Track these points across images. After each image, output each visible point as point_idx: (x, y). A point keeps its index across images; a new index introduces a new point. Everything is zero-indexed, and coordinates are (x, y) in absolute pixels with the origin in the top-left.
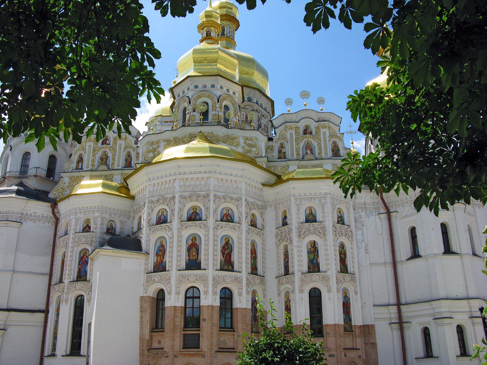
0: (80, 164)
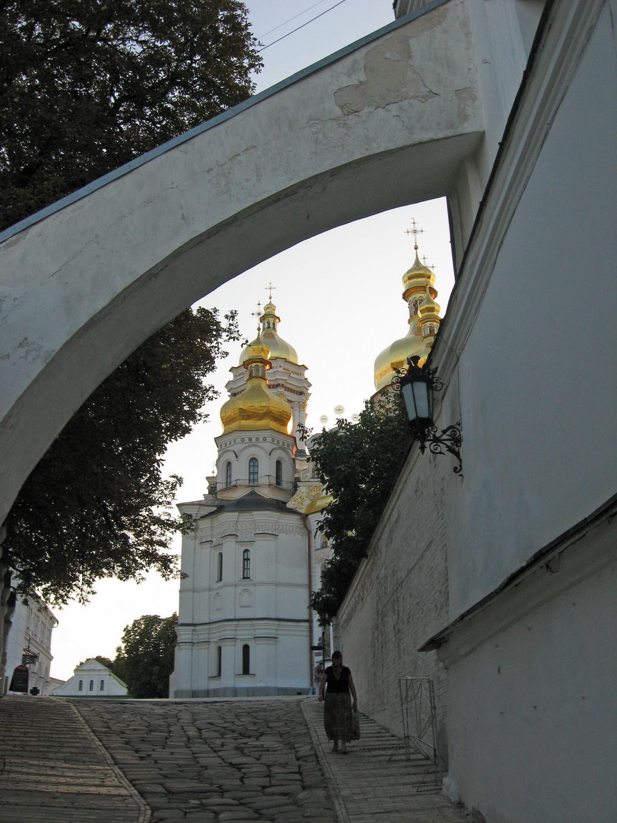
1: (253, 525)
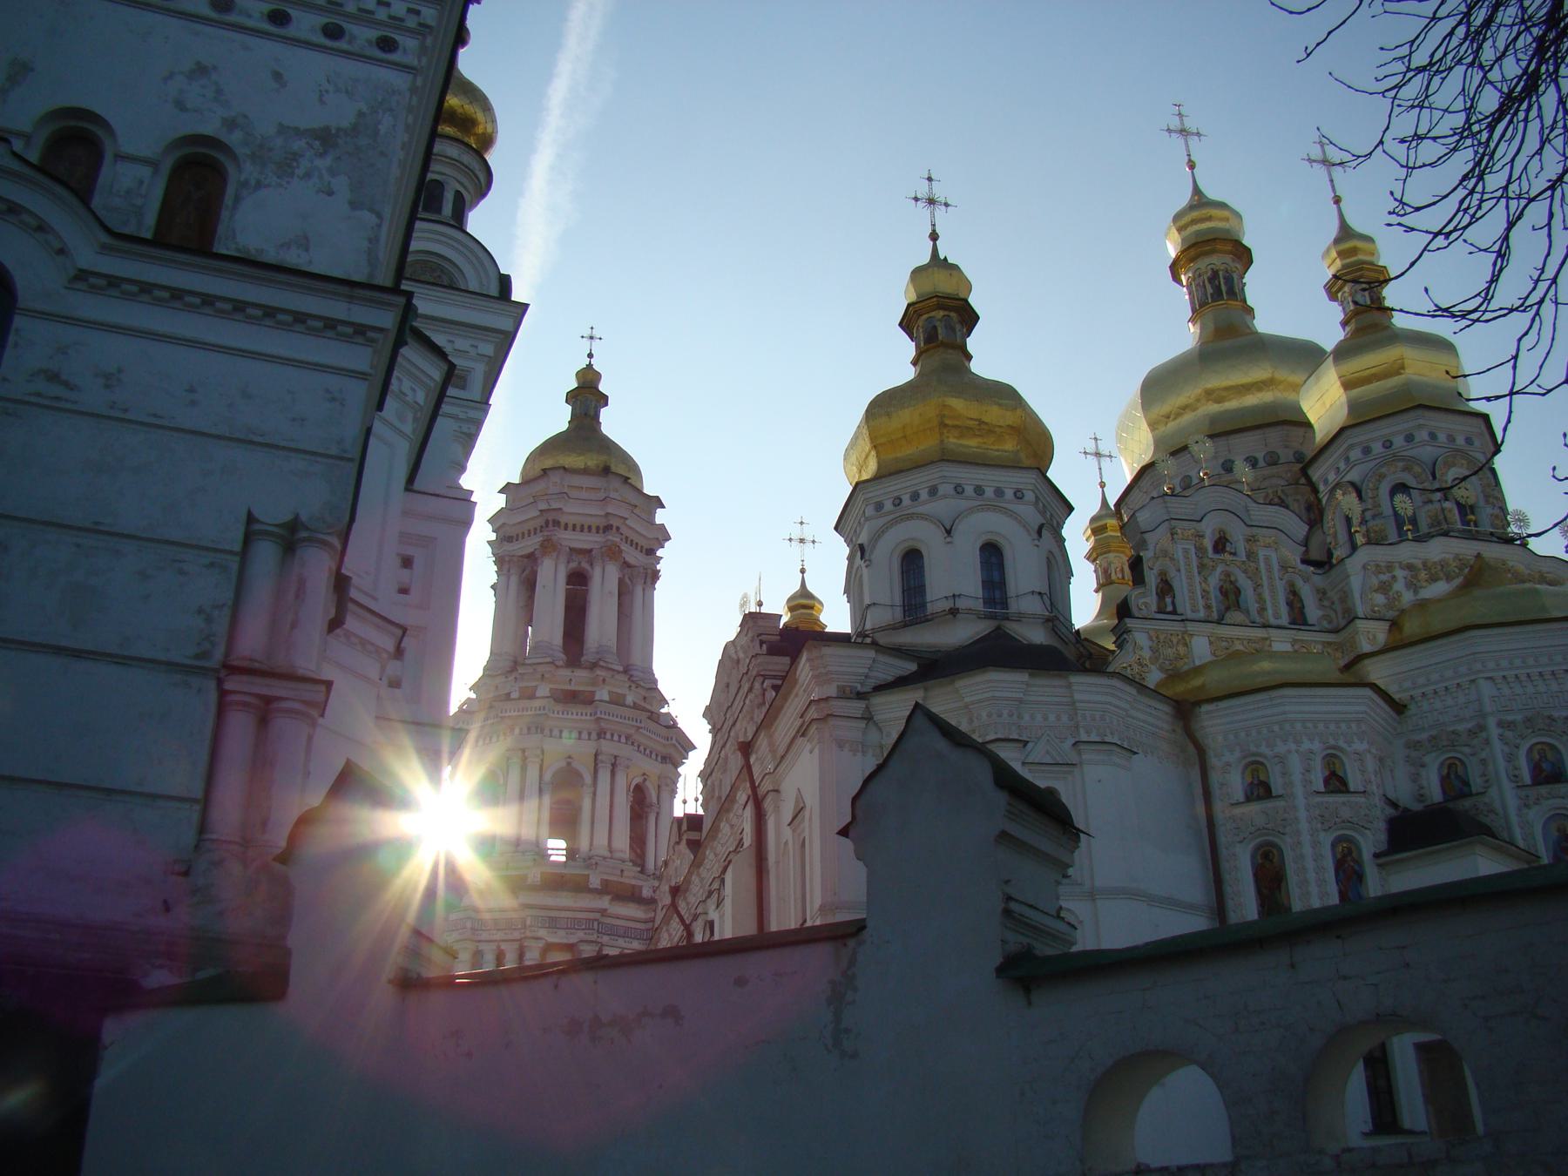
0: (1168, 600)
1: (1065, 718)
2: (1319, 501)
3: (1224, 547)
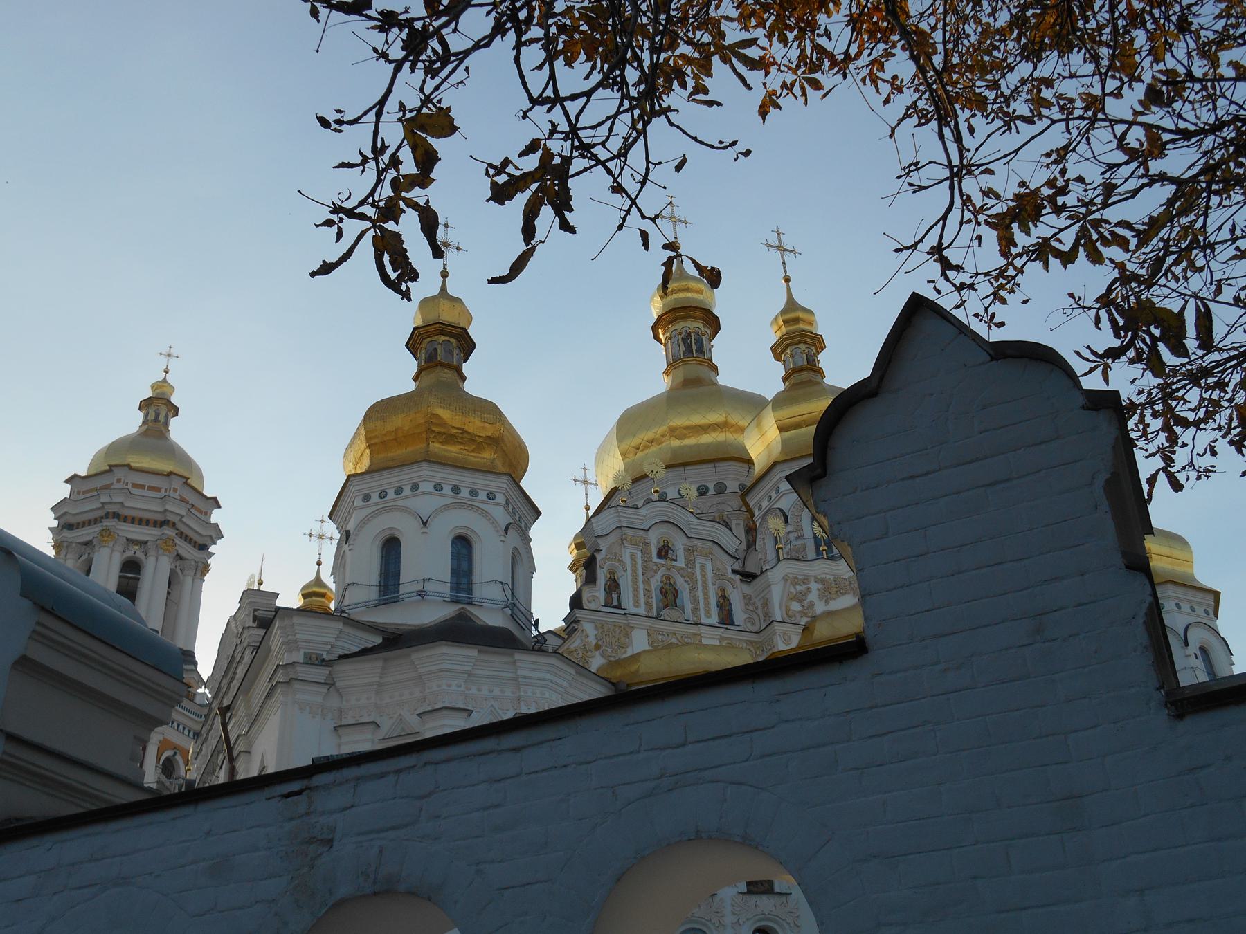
0: (614, 596)
1: (508, 693)
2: (754, 523)
3: (667, 552)
